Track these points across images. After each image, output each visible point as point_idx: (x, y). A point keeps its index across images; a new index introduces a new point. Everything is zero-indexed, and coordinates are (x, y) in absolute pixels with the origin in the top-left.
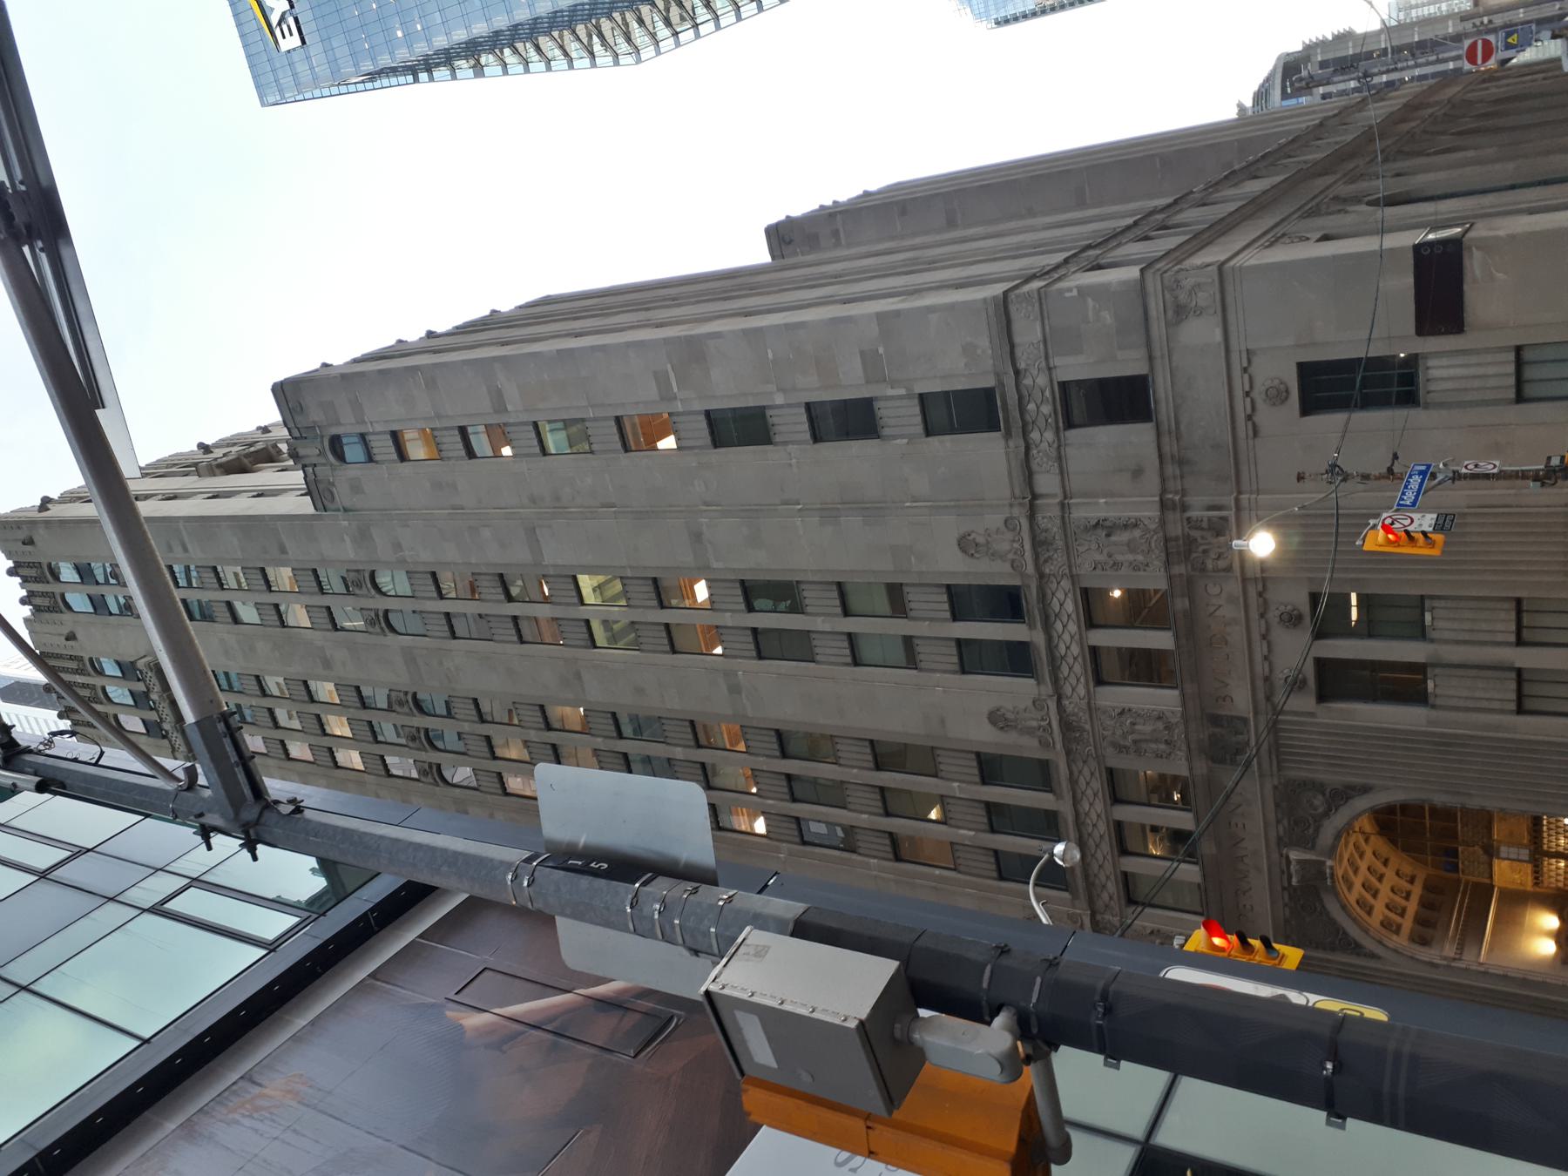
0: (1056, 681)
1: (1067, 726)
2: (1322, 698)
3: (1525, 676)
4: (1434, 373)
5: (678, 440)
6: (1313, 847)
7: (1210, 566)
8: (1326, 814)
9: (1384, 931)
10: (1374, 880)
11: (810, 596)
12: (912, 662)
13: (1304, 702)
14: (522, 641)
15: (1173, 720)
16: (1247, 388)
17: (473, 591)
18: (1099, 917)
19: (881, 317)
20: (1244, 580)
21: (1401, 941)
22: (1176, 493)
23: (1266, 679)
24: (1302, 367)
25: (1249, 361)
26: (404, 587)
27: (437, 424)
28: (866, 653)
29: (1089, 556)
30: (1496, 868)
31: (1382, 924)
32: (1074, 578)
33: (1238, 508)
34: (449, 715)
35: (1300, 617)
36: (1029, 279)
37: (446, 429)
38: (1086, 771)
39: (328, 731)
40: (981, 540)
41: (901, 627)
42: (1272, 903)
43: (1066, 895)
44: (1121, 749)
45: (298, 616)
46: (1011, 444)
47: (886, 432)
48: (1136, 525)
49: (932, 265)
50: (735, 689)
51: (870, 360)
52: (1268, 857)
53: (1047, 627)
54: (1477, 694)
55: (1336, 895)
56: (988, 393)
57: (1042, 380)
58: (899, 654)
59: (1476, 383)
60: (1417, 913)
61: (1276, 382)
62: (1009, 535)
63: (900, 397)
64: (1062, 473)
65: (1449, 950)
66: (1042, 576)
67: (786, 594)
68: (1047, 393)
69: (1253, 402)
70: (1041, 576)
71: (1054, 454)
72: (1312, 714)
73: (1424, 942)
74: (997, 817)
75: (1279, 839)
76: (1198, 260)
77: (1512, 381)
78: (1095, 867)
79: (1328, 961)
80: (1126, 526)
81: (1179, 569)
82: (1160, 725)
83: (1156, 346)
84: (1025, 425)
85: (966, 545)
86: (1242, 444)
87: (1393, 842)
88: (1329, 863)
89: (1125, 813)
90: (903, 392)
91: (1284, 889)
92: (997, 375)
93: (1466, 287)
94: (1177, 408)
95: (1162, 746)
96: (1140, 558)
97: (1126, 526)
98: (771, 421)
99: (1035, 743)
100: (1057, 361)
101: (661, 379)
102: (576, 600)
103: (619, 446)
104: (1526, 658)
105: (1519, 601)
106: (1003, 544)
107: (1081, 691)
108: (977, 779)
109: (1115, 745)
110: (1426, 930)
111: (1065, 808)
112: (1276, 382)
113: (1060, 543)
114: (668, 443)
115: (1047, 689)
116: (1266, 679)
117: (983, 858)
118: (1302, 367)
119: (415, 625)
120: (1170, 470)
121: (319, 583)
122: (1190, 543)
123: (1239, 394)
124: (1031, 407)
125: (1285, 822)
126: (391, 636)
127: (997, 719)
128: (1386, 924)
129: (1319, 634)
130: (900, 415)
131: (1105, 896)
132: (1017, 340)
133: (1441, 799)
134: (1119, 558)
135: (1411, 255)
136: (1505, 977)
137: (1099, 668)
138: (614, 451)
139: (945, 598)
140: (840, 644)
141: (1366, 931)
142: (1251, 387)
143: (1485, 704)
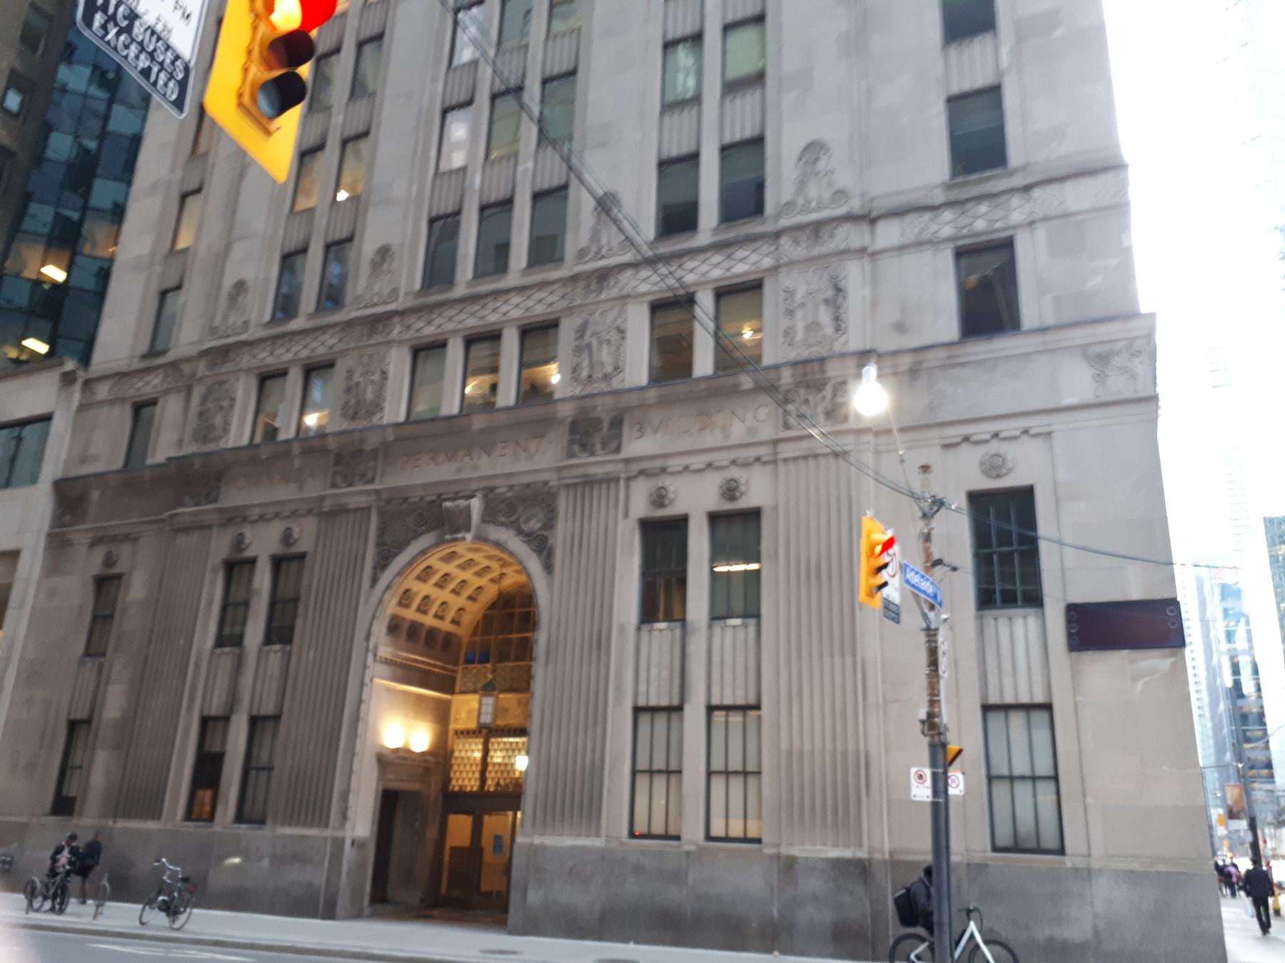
1: (603, 276)
2: (647, 526)
3: (674, 716)
4: (1019, 625)
7: (790, 407)
8: (520, 532)
9: (401, 590)
10: (452, 585)
12: (670, 106)
13: (640, 507)
16: (1003, 435)
21: (391, 607)
25: (1036, 435)
31: (408, 590)
32: (775, 269)
42: (425, 486)
43: (417, 285)
44: (581, 331)
47: (953, 51)
48: (838, 329)
52: (470, 480)
54: (654, 671)
57: (1017, 217)
59: (1007, 666)
61: (1010, 465)
65: (386, 651)
66: (777, 235)
68: (998, 225)
69: (986, 441)
70: (777, 235)
71: (926, 236)
72: (626, 514)
73: (394, 627)
74: (497, 210)
75: (492, 489)
77: (1009, 699)
80: (837, 319)
81: (787, 377)
82: (609, 369)
83: (1061, 335)
85: (814, 150)
86: (936, 433)
88: (469, 536)
90: (1005, 61)
91: (439, 496)
92: (1025, 167)
94: (979, 363)
95: (585, 373)
96: (799, 337)
100: (1041, 231)
104: (694, 714)
106: (814, 191)
107: (644, 288)
112: (1010, 465)
116: (663, 470)
117: (451, 202)
122: (819, 386)
124: (983, 208)
125: (509, 494)
129: (715, 518)
130: (974, 65)
131: (420, 324)
134: (799, 315)
135: (1171, 596)
136: (360, 701)
137: (672, 308)
141: (400, 573)
142: (1005, 439)
143: (643, 676)
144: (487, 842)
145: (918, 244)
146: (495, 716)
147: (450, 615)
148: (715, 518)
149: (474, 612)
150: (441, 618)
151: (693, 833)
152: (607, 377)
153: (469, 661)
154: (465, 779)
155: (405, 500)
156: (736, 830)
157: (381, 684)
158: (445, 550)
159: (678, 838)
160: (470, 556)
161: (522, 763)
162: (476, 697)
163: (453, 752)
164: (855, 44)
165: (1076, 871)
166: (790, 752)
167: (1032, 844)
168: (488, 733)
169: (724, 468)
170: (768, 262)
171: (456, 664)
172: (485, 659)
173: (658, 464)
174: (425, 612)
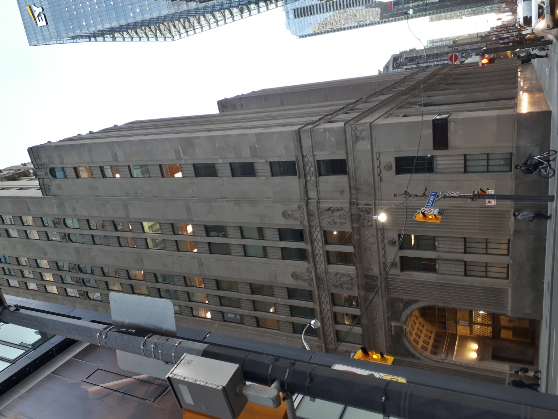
0: (314, 263)
1: (318, 278)
2: (402, 269)
3: (467, 263)
4: (438, 162)
5: (183, 174)
6: (399, 321)
7: (366, 224)
8: (404, 310)
10: (419, 333)
11: (230, 231)
12: (265, 255)
13: (396, 271)
14: (120, 246)
15: (354, 277)
17: (103, 227)
18: (327, 346)
19: (256, 134)
20: (377, 229)
21: (428, 353)
22: (355, 199)
23: (384, 263)
24: (396, 158)
25: (379, 156)
26: (76, 225)
27: (91, 165)
28: (250, 251)
29: (326, 220)
30: (458, 328)
32: (321, 227)
33: (375, 205)
34: (92, 273)
35: (395, 242)
36: (309, 124)
37: (95, 167)
38: (324, 295)
39: (44, 278)
40: (290, 213)
41: (262, 243)
42: (386, 341)
43: (317, 338)
44: (336, 287)
45: (34, 235)
46: (301, 180)
47: (258, 174)
49: (275, 118)
50: (201, 265)
51: (253, 149)
52: (385, 325)
53: (312, 244)
54: (452, 269)
55: (407, 337)
56: (293, 163)
57: (311, 159)
58: (261, 253)
59: (452, 166)
60: (433, 344)
62: (300, 212)
63: (263, 163)
64: (317, 191)
65: (443, 356)
66: (310, 226)
67: (221, 230)
68: (313, 164)
70: (310, 226)
71: (314, 184)
72: (399, 275)
73: (434, 353)
74: (294, 311)
75: (388, 318)
76: (363, 121)
78: (327, 328)
79: (404, 361)
81: (355, 225)
82: (349, 278)
83: (349, 149)
84: (305, 174)
85: (284, 214)
86: (377, 184)
87: (425, 319)
88: (404, 327)
89: (337, 309)
90: (264, 161)
92: (296, 157)
93: (449, 134)
95: (350, 286)
96: (343, 221)
97: (338, 210)
98: (217, 168)
99: (307, 284)
100: (316, 153)
101: (177, 152)
102: (142, 231)
103: (160, 175)
105: (465, 239)
107: (323, 266)
108: (287, 297)
109: (334, 285)
110: (436, 350)
111: (317, 307)
113: (316, 215)
114: (179, 175)
115: (312, 265)
116: (384, 263)
118: (396, 158)
119: (80, 239)
120: (353, 191)
121: (43, 222)
122: (359, 216)
123: (376, 167)
124: (307, 168)
125: (390, 312)
126: (70, 243)
127: (294, 276)
128: (423, 348)
129: (401, 248)
130: (263, 169)
131: (330, 338)
132: (303, 145)
133: (441, 305)
134: (336, 221)
137: (329, 258)
138: (159, 177)
139: (277, 233)
140: (240, 249)
141: (416, 350)
142: (380, 164)
143: (454, 273)
144: (511, 325)
145: (317, 186)
146: (466, 320)
147: (429, 334)
148: (401, 248)
149: (427, 326)
150: (430, 337)
151: (506, 260)
152: (352, 279)
153: (445, 328)
154: (488, 331)
155: (390, 347)
156: (505, 246)
157: (454, 358)
158: (409, 334)
159: (508, 265)
160: (410, 326)
161: (481, 312)
162: (458, 326)
163: (478, 335)
164: (253, 202)
165: (517, 150)
166: (480, 230)
167: (509, 161)
168: (471, 323)
169: (384, 244)
170: (318, 229)
171: (446, 333)
172: (445, 323)
173: (382, 265)
174: (429, 343)
